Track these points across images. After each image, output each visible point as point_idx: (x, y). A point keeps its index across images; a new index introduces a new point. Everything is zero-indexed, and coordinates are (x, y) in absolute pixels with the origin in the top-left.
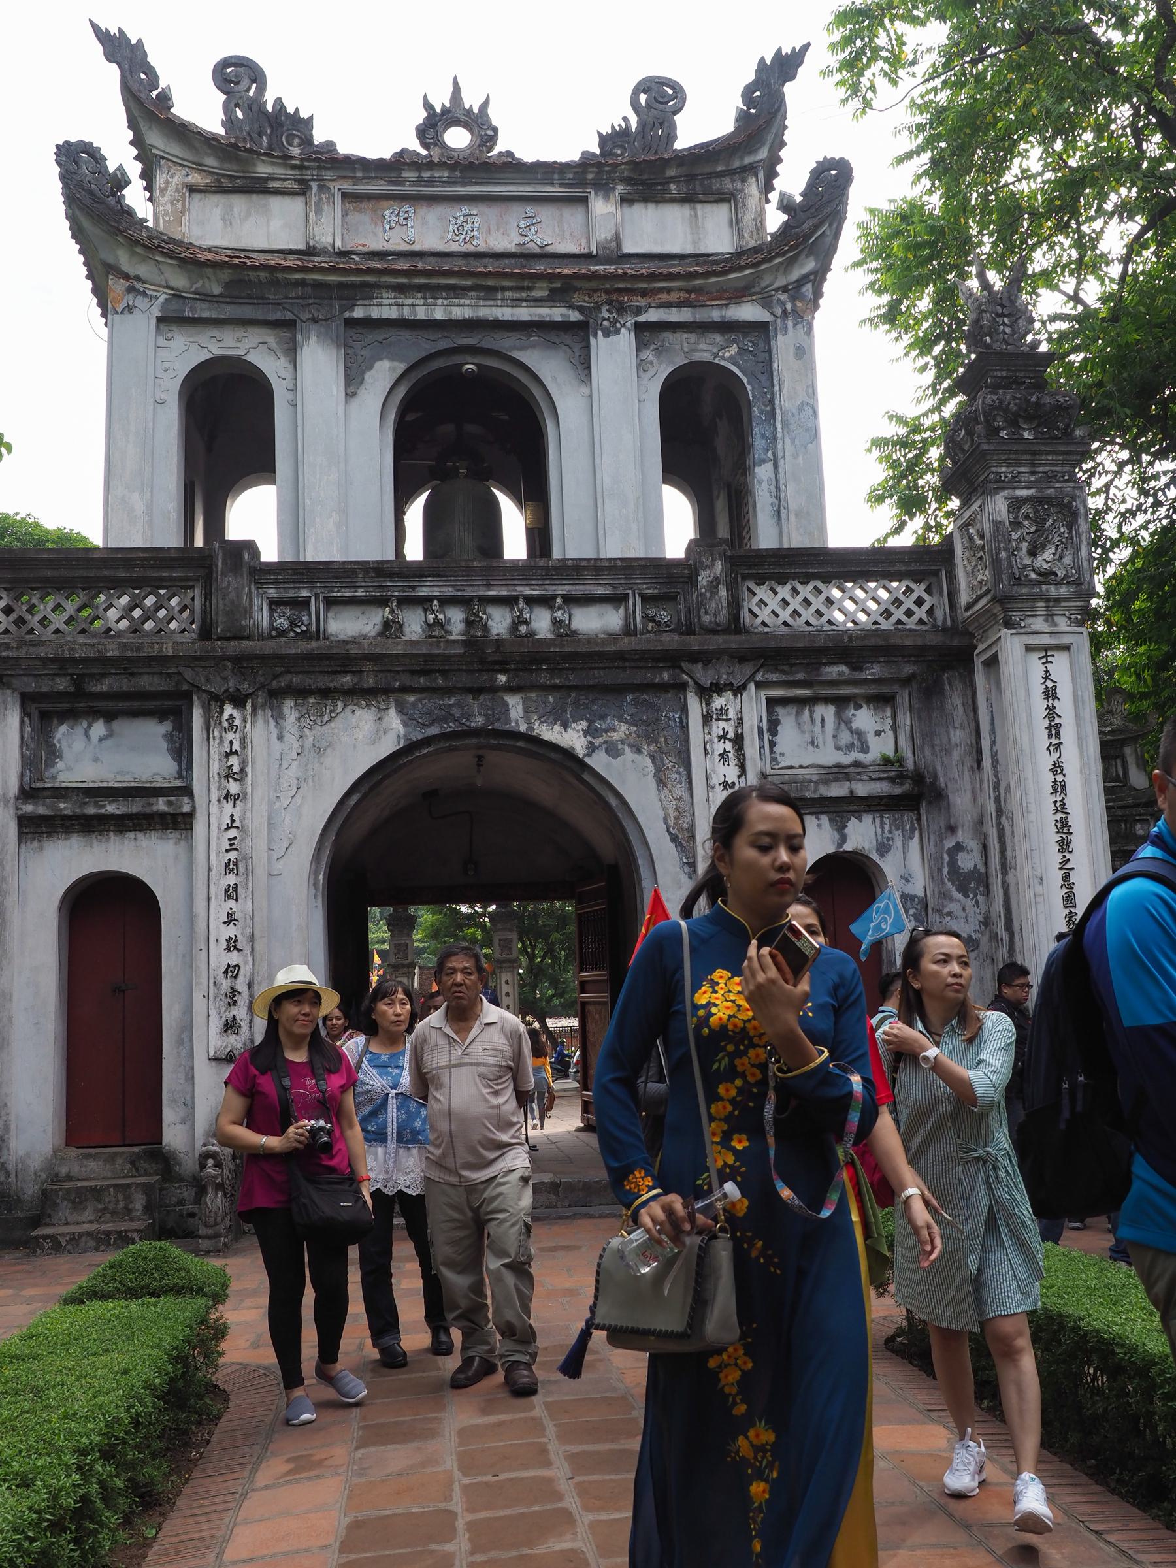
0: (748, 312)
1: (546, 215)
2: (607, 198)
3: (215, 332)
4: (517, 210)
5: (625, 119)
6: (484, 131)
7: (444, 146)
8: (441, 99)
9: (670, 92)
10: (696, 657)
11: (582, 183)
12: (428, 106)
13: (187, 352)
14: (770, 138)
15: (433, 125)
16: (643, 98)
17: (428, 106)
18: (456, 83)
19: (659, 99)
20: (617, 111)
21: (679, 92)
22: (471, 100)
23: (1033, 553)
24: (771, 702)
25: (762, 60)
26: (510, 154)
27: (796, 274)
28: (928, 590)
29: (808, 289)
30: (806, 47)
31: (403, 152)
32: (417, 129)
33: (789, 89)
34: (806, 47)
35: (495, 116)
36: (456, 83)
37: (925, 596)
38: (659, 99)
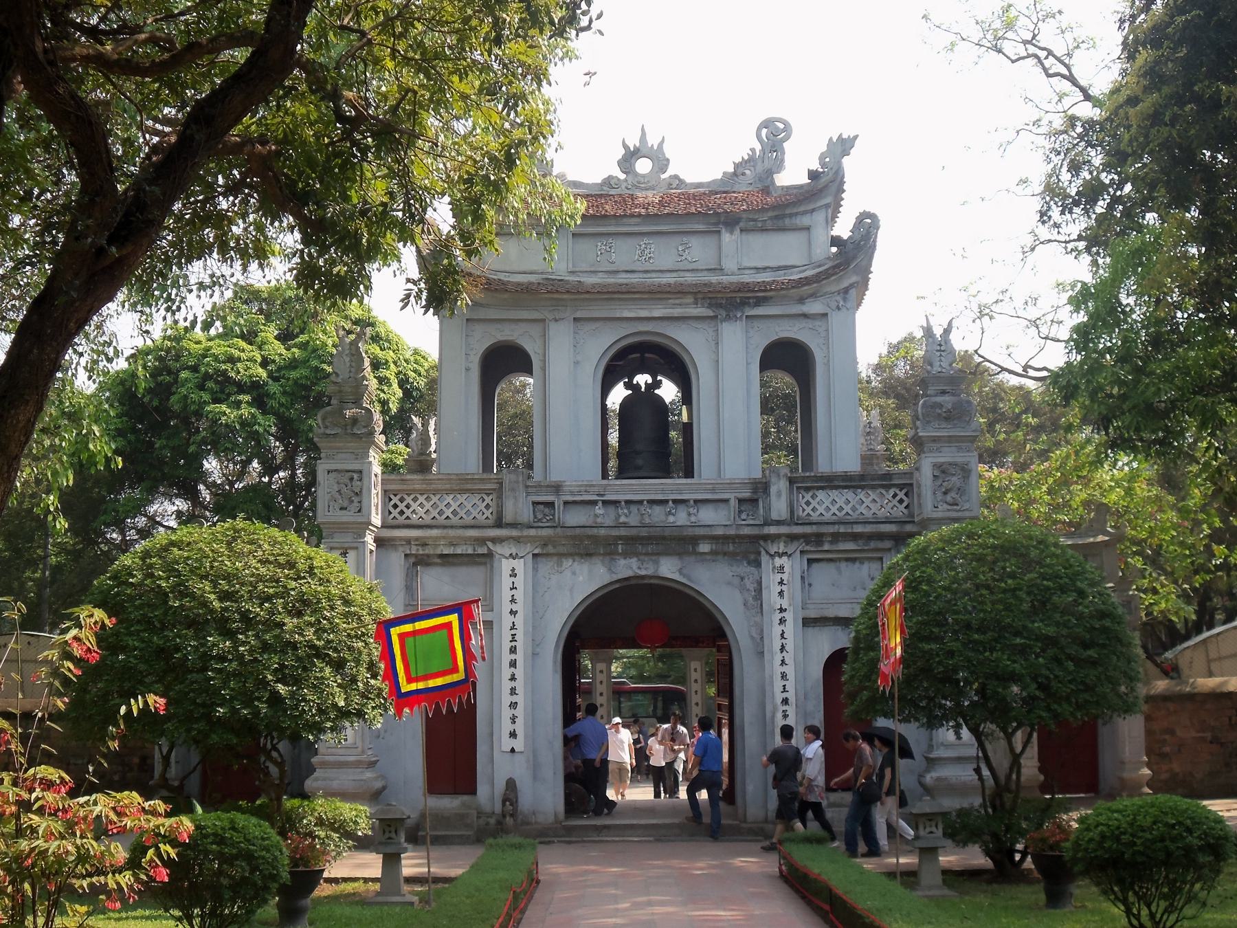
0: (814, 307)
1: (694, 242)
2: (731, 233)
3: (499, 326)
4: (676, 240)
5: (753, 150)
6: (661, 163)
7: (636, 174)
8: (633, 142)
9: (781, 126)
10: (766, 538)
11: (716, 224)
12: (625, 146)
13: (484, 339)
14: (833, 188)
15: (629, 157)
16: (764, 131)
17: (625, 146)
18: (643, 129)
19: (774, 135)
20: (745, 144)
21: (787, 128)
22: (653, 141)
23: (945, 493)
24: (809, 560)
25: (831, 139)
26: (676, 177)
27: (845, 284)
28: (906, 494)
29: (853, 292)
30: (856, 137)
31: (610, 177)
32: (619, 163)
33: (846, 161)
34: (856, 137)
35: (668, 152)
36: (643, 129)
37: (905, 498)
38: (774, 135)
